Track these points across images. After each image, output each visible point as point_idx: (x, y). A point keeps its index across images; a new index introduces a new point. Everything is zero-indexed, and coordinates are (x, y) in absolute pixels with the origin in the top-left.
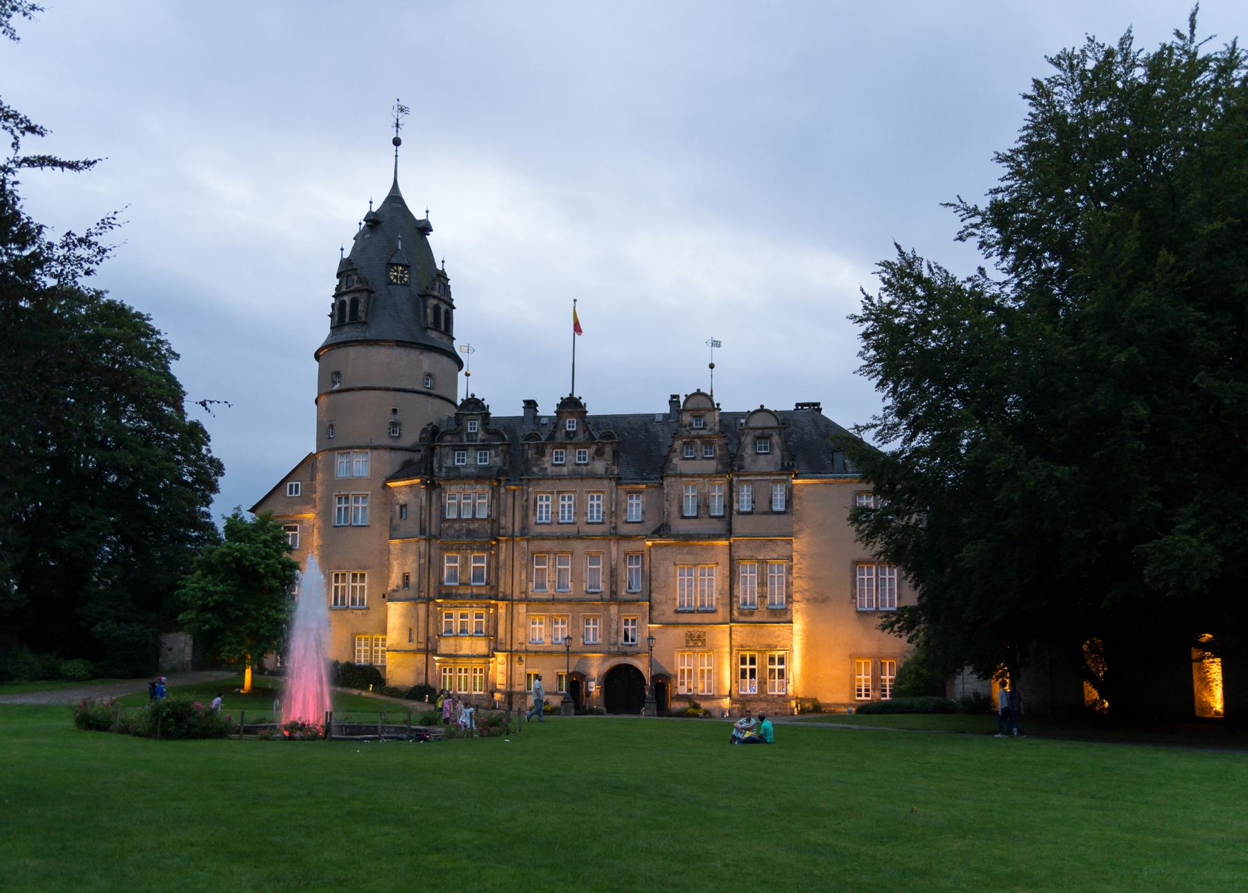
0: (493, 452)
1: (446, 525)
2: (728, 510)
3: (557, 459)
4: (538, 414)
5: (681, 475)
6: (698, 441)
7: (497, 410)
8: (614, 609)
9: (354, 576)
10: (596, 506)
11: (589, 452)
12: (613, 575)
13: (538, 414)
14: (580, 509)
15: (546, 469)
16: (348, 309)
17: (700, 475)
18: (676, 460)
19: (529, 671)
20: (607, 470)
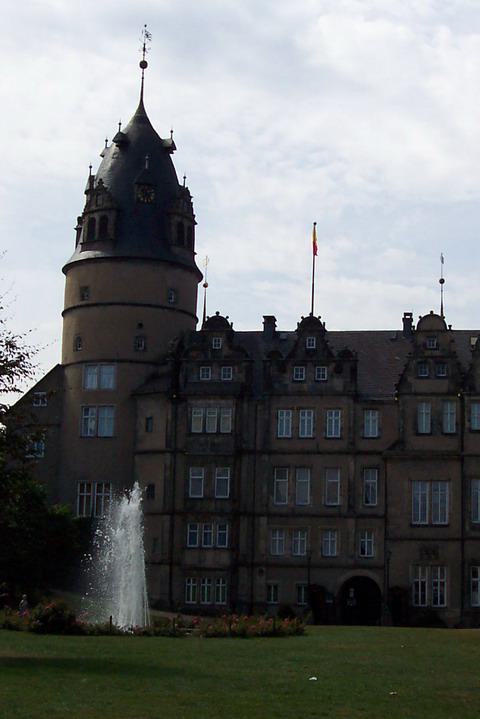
0: (236, 368)
1: (192, 439)
2: (460, 427)
3: (297, 377)
4: (277, 329)
5: (416, 394)
6: (431, 361)
7: (238, 327)
8: (351, 522)
9: (99, 486)
10: (335, 423)
11: (326, 371)
12: (351, 489)
13: (277, 329)
14: (320, 425)
15: (286, 386)
16: (97, 227)
17: (433, 394)
18: (410, 379)
19: (270, 582)
20: (345, 387)
